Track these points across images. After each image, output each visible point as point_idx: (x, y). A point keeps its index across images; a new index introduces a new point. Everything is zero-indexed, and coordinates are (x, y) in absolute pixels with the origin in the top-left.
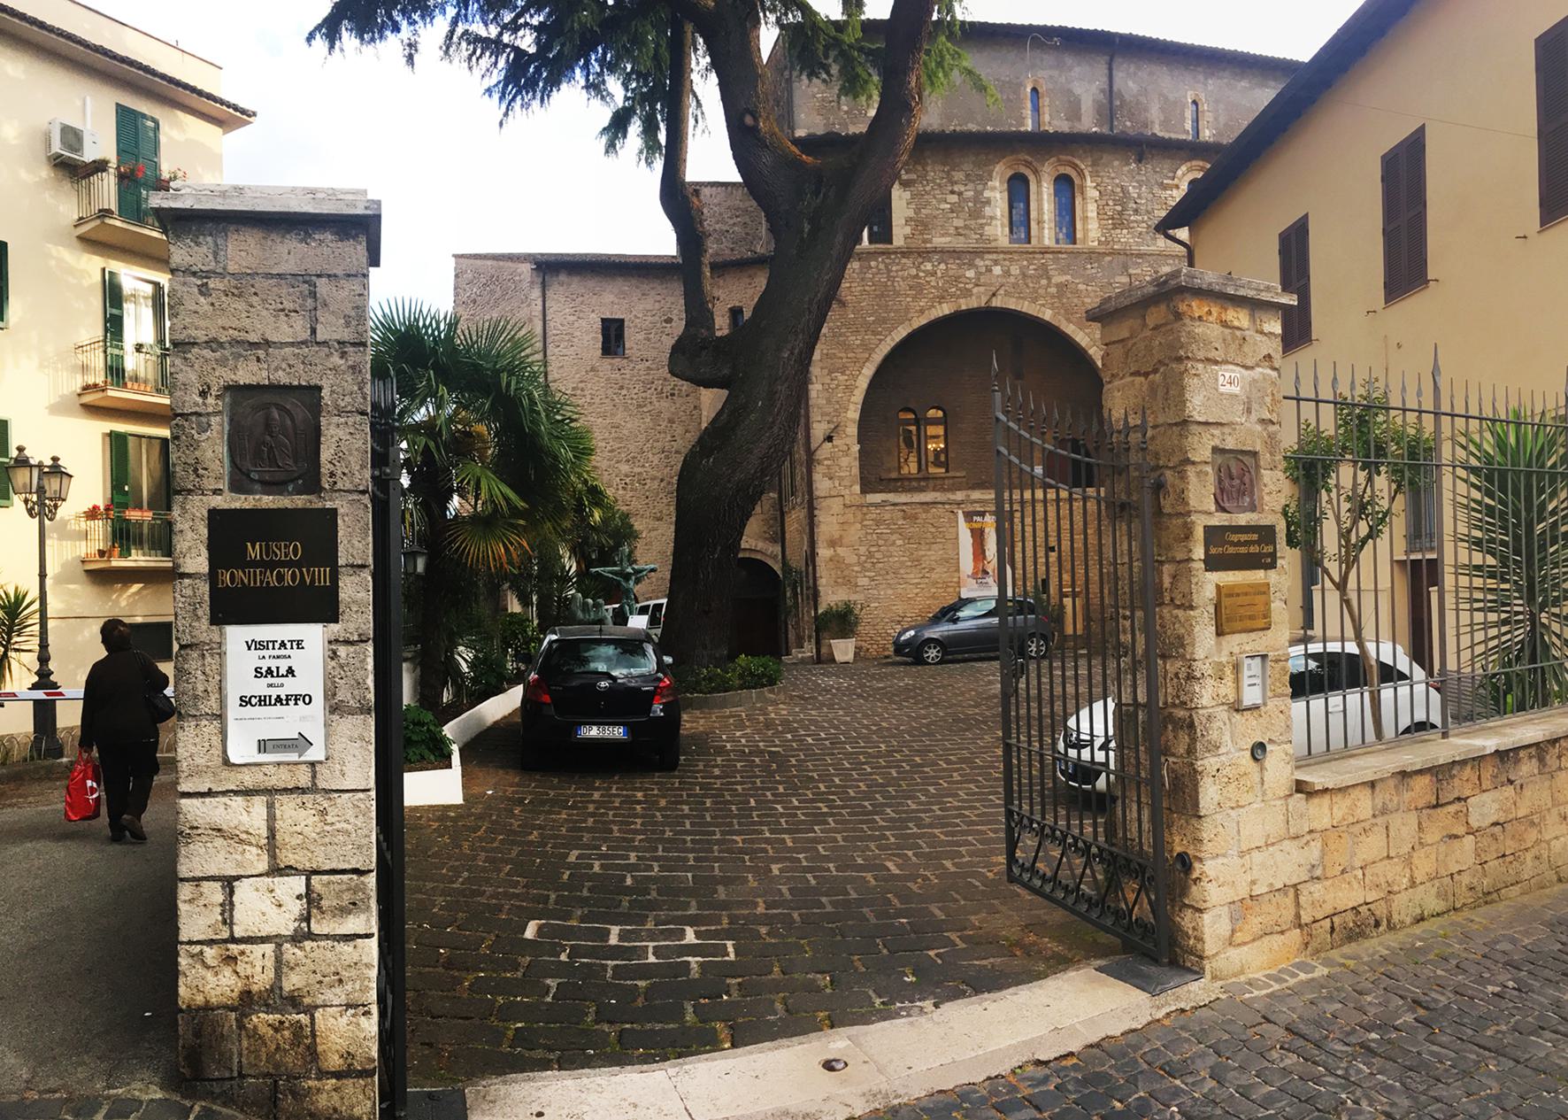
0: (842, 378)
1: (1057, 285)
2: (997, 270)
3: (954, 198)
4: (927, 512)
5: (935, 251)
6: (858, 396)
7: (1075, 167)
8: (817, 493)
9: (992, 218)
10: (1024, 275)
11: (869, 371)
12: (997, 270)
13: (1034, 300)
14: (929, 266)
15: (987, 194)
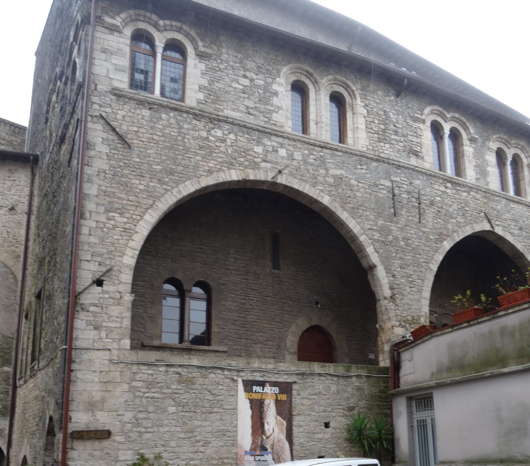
0: (119, 219)
1: (333, 176)
2: (283, 152)
3: (247, 82)
4: (204, 377)
5: (226, 120)
6: (138, 241)
7: (347, 87)
8: (78, 344)
9: (279, 108)
10: (305, 162)
11: (151, 219)
12: (283, 152)
13: (314, 185)
14: (219, 133)
15: (275, 87)
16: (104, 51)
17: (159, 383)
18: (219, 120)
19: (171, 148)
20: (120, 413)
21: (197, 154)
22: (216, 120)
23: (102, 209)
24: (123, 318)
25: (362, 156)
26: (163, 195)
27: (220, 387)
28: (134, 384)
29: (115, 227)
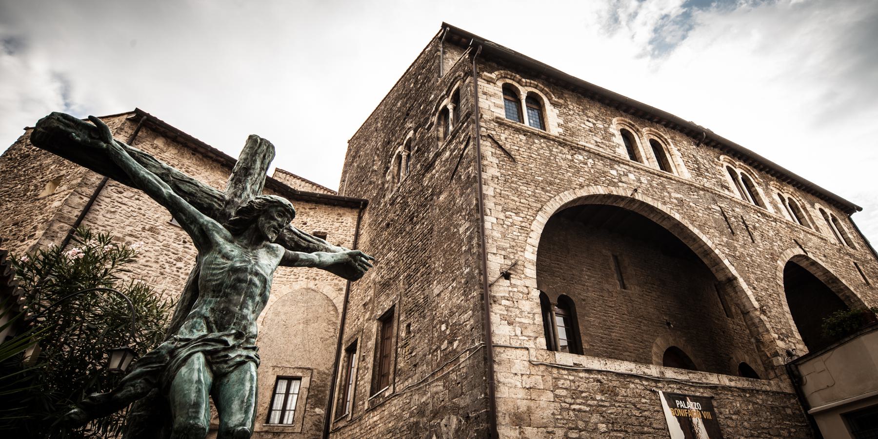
2: (632, 176)
6: (535, 239)
7: (660, 137)
8: (495, 340)
16: (485, 93)
17: (582, 392)
18: (579, 148)
19: (547, 165)
20: (550, 429)
21: (568, 171)
22: (576, 149)
23: (500, 208)
24: (534, 314)
25: (692, 185)
26: (548, 201)
27: (644, 400)
28: (558, 392)
29: (513, 224)
